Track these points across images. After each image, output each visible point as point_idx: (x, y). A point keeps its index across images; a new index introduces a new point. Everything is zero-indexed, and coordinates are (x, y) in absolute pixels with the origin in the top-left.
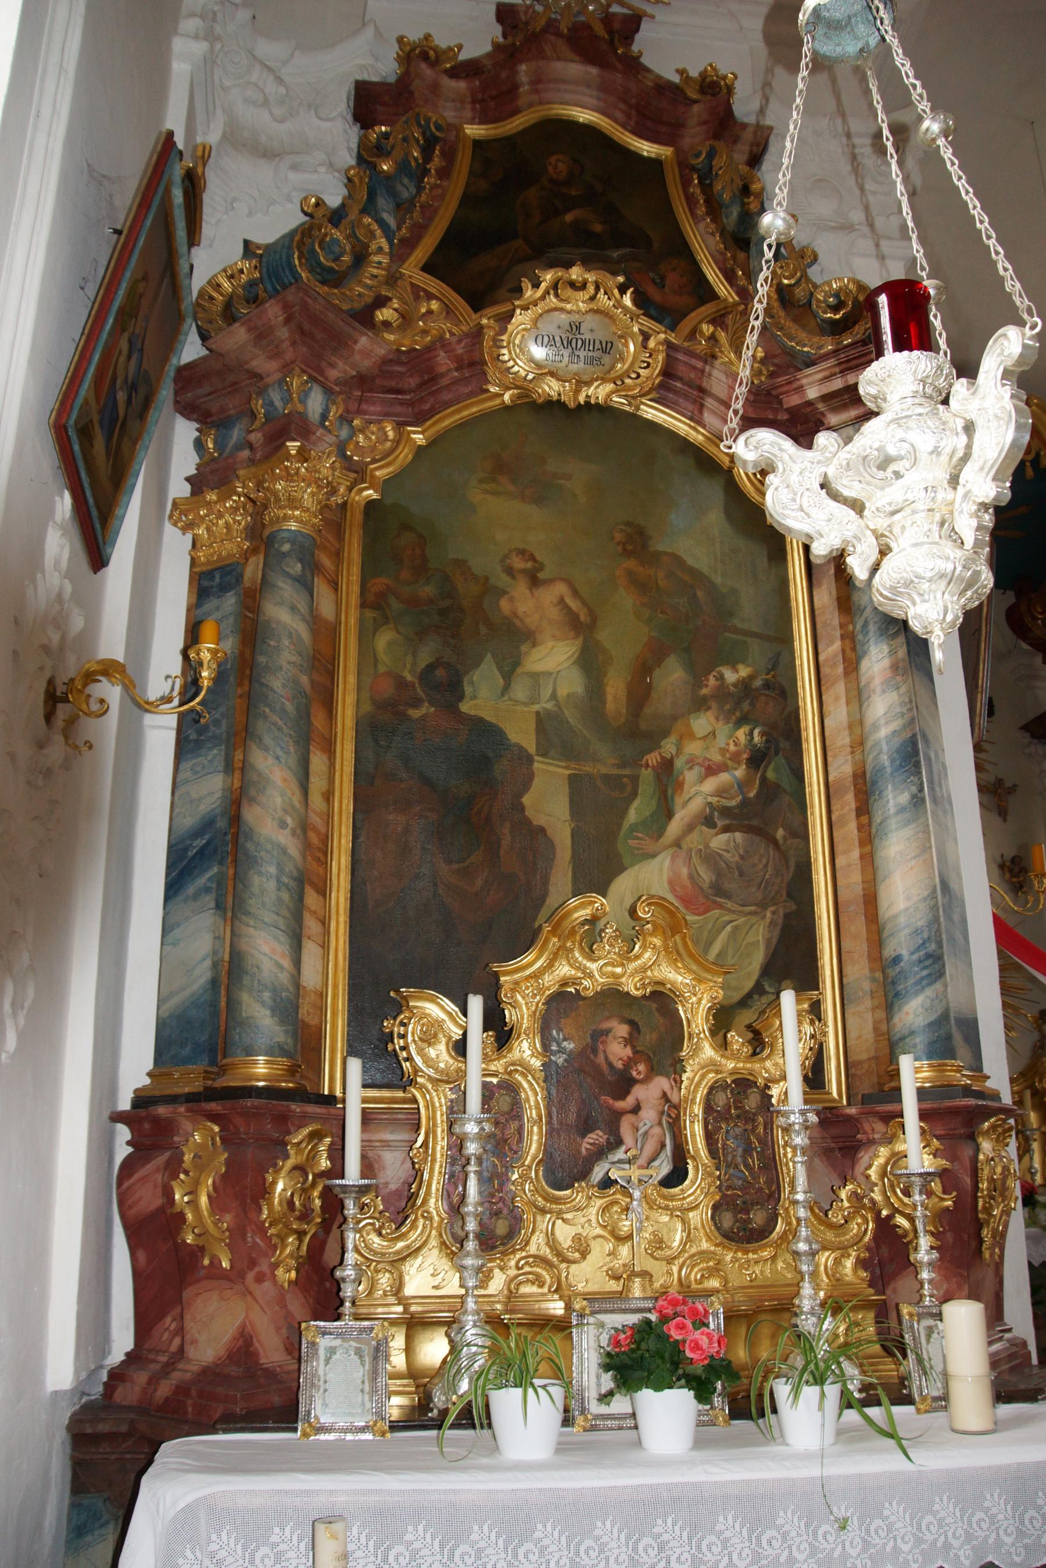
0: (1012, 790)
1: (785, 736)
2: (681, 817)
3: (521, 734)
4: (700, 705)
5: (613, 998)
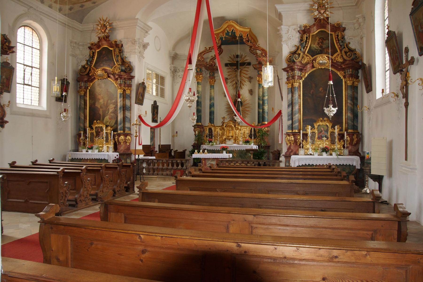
0: (252, 78)
1: (117, 105)
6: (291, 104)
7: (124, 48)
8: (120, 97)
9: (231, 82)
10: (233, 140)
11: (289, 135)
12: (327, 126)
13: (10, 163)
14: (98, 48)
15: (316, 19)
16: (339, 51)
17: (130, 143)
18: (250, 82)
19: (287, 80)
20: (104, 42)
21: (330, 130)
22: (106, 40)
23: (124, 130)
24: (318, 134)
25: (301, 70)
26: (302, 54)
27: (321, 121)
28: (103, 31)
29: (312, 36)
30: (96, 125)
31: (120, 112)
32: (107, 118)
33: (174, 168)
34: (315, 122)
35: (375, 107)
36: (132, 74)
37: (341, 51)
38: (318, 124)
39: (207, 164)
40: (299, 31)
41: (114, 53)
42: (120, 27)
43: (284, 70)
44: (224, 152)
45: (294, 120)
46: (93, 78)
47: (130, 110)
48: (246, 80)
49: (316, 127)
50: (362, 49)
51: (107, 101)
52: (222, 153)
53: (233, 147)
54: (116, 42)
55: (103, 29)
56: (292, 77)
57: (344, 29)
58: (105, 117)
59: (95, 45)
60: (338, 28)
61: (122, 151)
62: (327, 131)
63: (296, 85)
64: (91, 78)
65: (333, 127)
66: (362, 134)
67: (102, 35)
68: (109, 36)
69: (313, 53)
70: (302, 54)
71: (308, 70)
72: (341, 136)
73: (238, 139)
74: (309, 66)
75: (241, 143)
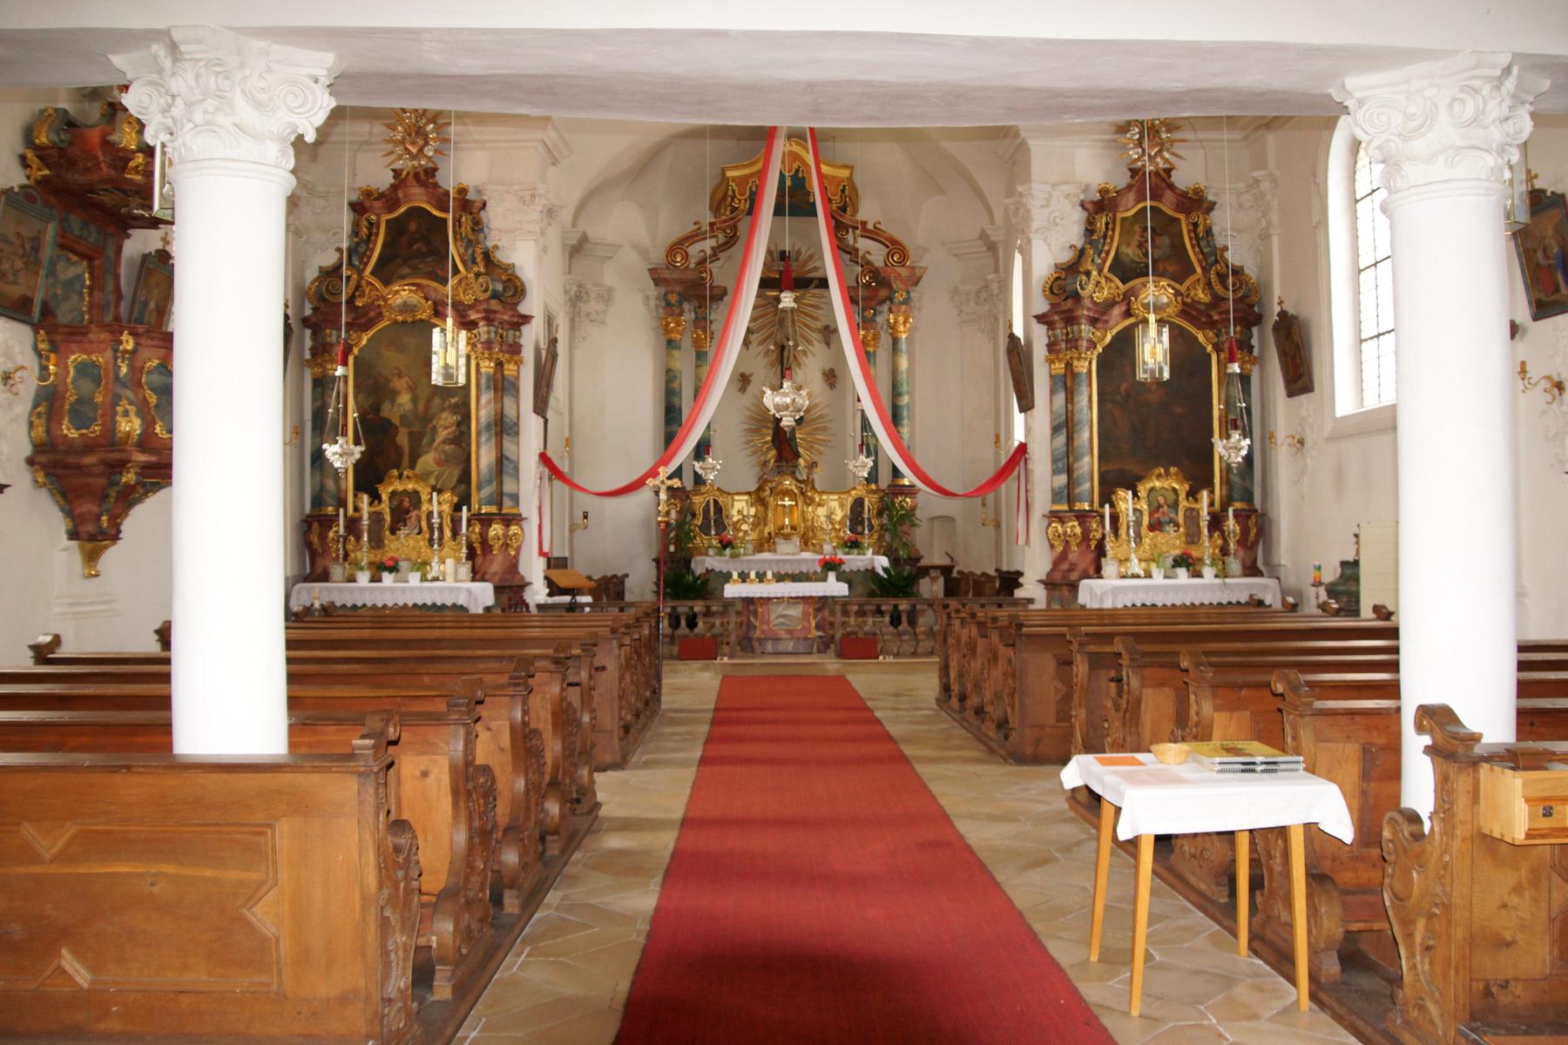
2: (439, 439)
3: (396, 421)
4: (444, 409)
5: (405, 492)
6: (1066, 425)
7: (491, 215)
8: (488, 387)
9: (761, 343)
10: (796, 540)
11: (1062, 521)
12: (1174, 490)
13: (157, 627)
14: (391, 210)
15: (1134, 172)
16: (1199, 270)
17: (518, 550)
18: (828, 344)
19: (1050, 351)
20: (416, 190)
21: (1184, 503)
22: (423, 184)
23: (500, 506)
24: (1151, 515)
25: (1093, 322)
26: (1095, 273)
27: (1159, 476)
28: (414, 150)
29: (1123, 219)
30: (391, 484)
31: (488, 440)
32: (428, 460)
33: (679, 632)
34: (1140, 478)
35: (1331, 439)
36: (523, 309)
37: (1205, 270)
38: (1149, 485)
39: (773, 616)
40: (1082, 205)
41: (455, 233)
42: (477, 142)
43: (1041, 319)
44: (832, 576)
45: (1076, 474)
46: (372, 314)
47: (517, 434)
48: (814, 336)
49: (1142, 493)
50: (1265, 266)
51: (429, 400)
52: (825, 579)
53: (800, 561)
54: (462, 191)
55: (413, 143)
56: (1067, 341)
57: (1211, 206)
58: (419, 456)
59: (381, 196)
60: (1196, 203)
61: (497, 577)
62: (1175, 506)
63: (1081, 367)
64: (366, 314)
65: (1193, 494)
66: (1263, 515)
67: (405, 164)
68: (435, 169)
69: (1127, 271)
70: (1095, 273)
71: (1112, 323)
72: (1216, 522)
73: (814, 537)
74: (1117, 311)
75: (827, 548)
